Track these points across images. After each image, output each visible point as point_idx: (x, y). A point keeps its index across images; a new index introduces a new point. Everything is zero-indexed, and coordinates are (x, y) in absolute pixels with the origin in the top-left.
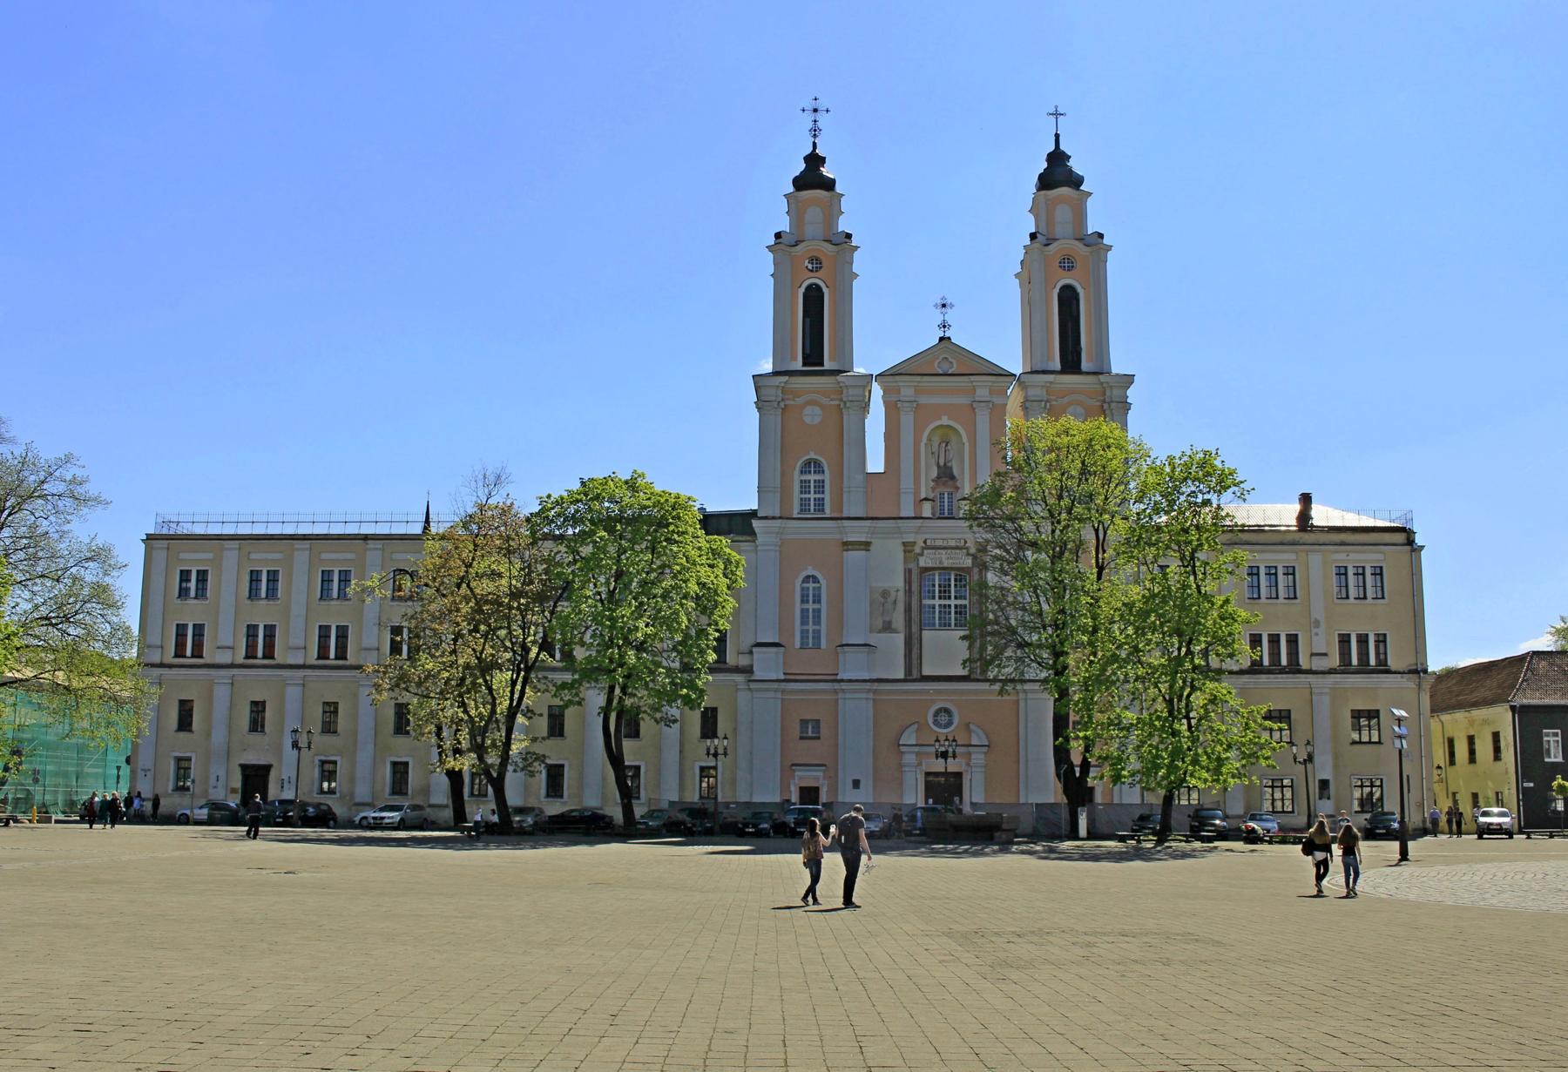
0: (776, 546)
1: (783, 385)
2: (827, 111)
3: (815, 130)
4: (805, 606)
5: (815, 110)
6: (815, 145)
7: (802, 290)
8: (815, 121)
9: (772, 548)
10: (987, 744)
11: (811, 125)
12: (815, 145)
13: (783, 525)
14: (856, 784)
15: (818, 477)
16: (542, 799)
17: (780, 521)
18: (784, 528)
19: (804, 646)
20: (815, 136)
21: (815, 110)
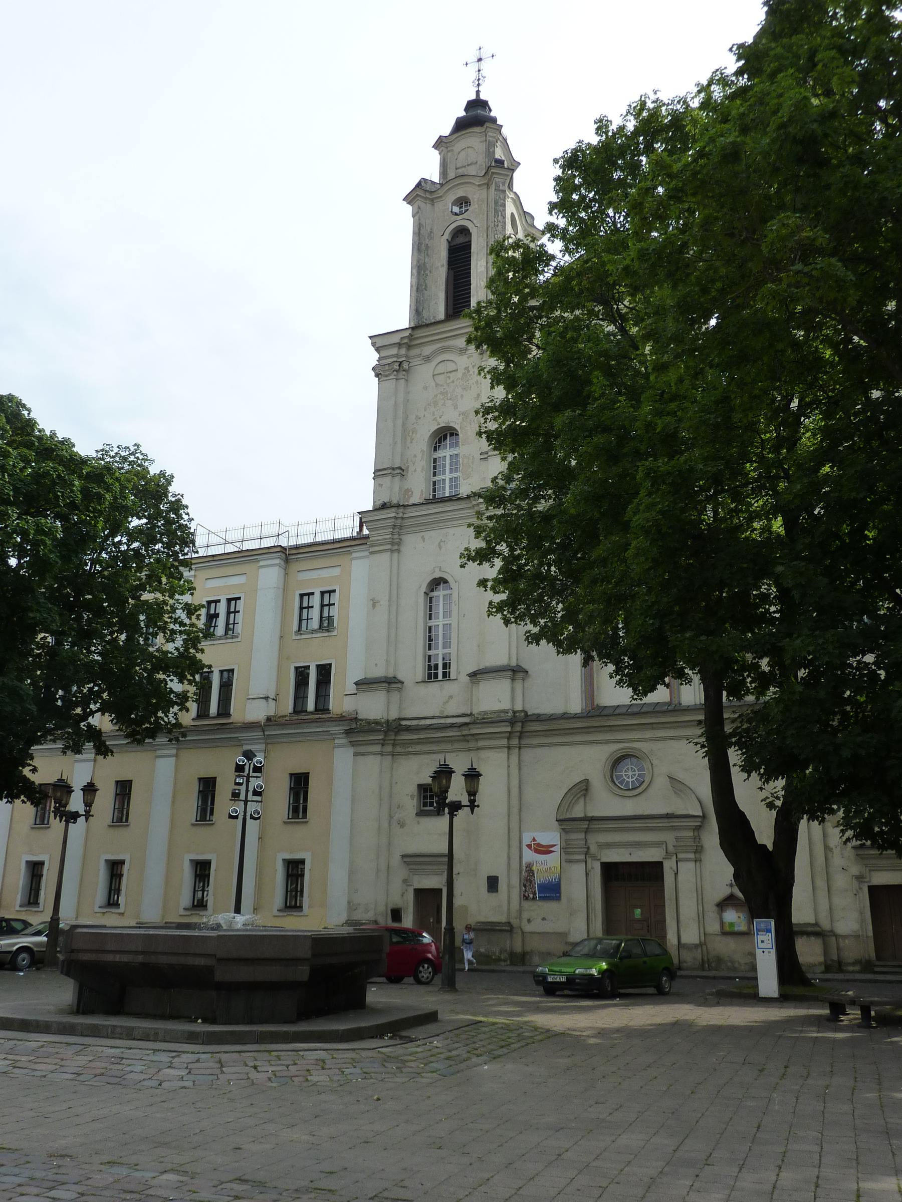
0: (393, 544)
1: (406, 341)
2: (493, 56)
3: (479, 80)
4: (432, 623)
5: (480, 60)
6: (478, 92)
7: (447, 236)
8: (479, 71)
9: (389, 547)
10: (701, 814)
11: (474, 75)
12: (478, 92)
13: (401, 515)
14: (493, 883)
15: (454, 451)
16: (18, 908)
17: (394, 510)
18: (402, 518)
19: (431, 675)
20: (479, 85)
21: (480, 60)
